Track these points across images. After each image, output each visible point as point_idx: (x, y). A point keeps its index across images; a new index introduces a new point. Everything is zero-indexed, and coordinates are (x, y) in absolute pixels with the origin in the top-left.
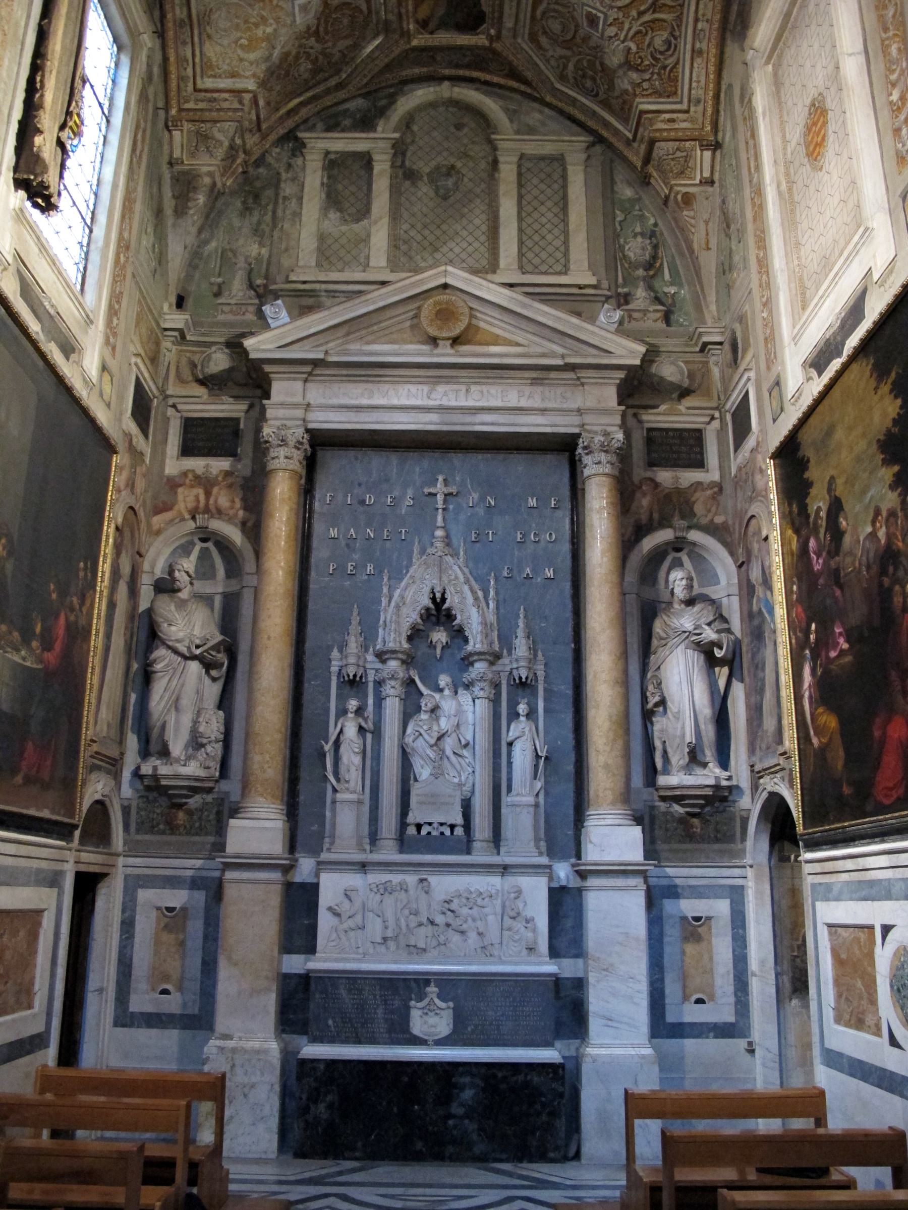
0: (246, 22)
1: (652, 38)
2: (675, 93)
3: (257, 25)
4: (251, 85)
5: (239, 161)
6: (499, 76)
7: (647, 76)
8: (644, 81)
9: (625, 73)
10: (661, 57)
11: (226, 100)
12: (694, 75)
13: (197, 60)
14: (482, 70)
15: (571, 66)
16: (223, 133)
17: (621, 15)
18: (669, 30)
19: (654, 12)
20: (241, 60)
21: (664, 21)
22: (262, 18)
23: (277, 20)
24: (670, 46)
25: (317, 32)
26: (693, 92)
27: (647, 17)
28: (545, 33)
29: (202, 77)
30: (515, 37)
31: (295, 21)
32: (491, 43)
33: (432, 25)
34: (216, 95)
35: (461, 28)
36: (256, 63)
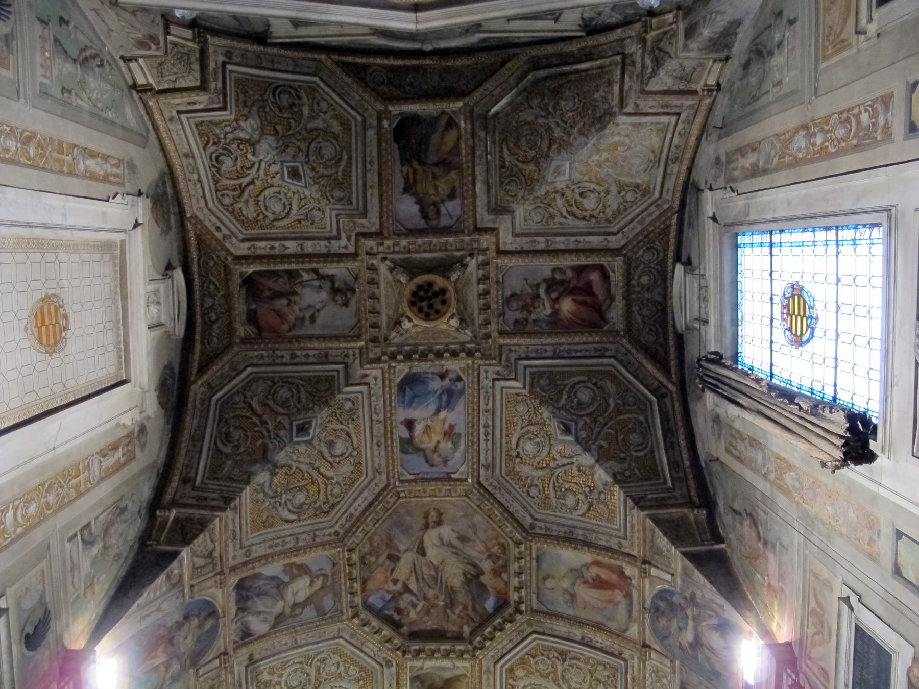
0: (616, 163)
1: (235, 165)
2: (197, 125)
3: (607, 160)
4: (621, 119)
5: (654, 33)
6: (375, 65)
7: (230, 136)
8: (231, 132)
9: (252, 136)
10: (221, 151)
11: (651, 107)
12: (184, 139)
13: (669, 136)
14: (393, 69)
15: (306, 110)
16: (664, 80)
17: (269, 180)
18: (222, 171)
19: (240, 185)
20: (627, 136)
21: (228, 178)
22: (600, 166)
23: (587, 164)
24: (217, 161)
25: (552, 141)
26: (180, 127)
27: (245, 181)
28: (336, 137)
29: (669, 124)
30: (364, 121)
31: (571, 164)
32: (386, 108)
33: (443, 122)
34: (660, 110)
35: (415, 119)
36: (613, 134)
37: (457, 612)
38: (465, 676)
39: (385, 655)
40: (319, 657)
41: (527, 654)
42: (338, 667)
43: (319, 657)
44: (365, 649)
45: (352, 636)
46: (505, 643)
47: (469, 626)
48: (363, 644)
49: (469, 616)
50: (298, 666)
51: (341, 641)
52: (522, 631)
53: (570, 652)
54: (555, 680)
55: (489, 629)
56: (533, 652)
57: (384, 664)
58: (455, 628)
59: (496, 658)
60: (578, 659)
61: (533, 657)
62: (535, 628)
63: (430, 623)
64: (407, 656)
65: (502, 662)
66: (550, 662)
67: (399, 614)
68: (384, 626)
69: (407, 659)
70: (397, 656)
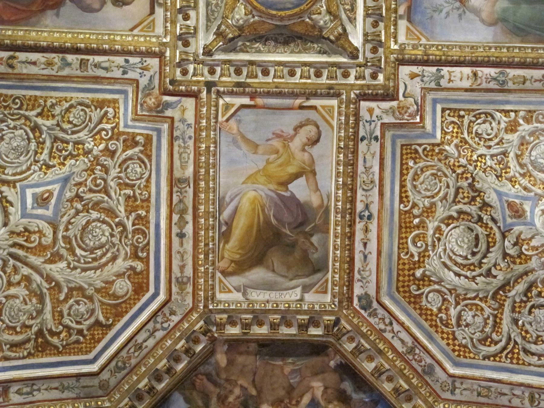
37: (237, 391)
38: (225, 273)
39: (372, 320)
40: (493, 349)
41: (109, 327)
42: (459, 317)
43: (493, 349)
44: (409, 340)
45: (429, 371)
46: (151, 343)
47: (217, 363)
48: (411, 351)
49: (216, 384)
50: (533, 348)
51: (452, 370)
52: (118, 369)
53: (30, 355)
54: (58, 286)
55: (180, 367)
56: (98, 333)
57: (375, 305)
58: (240, 359)
59: (166, 310)
60: (14, 346)
61: (97, 323)
62: (95, 381)
63: (287, 369)
64: (333, 318)
65: (154, 306)
66: (67, 321)
67: (344, 391)
68: (372, 379)
69: (331, 313)
70: (350, 322)
